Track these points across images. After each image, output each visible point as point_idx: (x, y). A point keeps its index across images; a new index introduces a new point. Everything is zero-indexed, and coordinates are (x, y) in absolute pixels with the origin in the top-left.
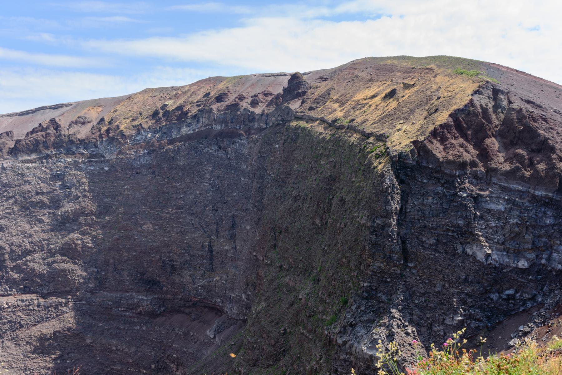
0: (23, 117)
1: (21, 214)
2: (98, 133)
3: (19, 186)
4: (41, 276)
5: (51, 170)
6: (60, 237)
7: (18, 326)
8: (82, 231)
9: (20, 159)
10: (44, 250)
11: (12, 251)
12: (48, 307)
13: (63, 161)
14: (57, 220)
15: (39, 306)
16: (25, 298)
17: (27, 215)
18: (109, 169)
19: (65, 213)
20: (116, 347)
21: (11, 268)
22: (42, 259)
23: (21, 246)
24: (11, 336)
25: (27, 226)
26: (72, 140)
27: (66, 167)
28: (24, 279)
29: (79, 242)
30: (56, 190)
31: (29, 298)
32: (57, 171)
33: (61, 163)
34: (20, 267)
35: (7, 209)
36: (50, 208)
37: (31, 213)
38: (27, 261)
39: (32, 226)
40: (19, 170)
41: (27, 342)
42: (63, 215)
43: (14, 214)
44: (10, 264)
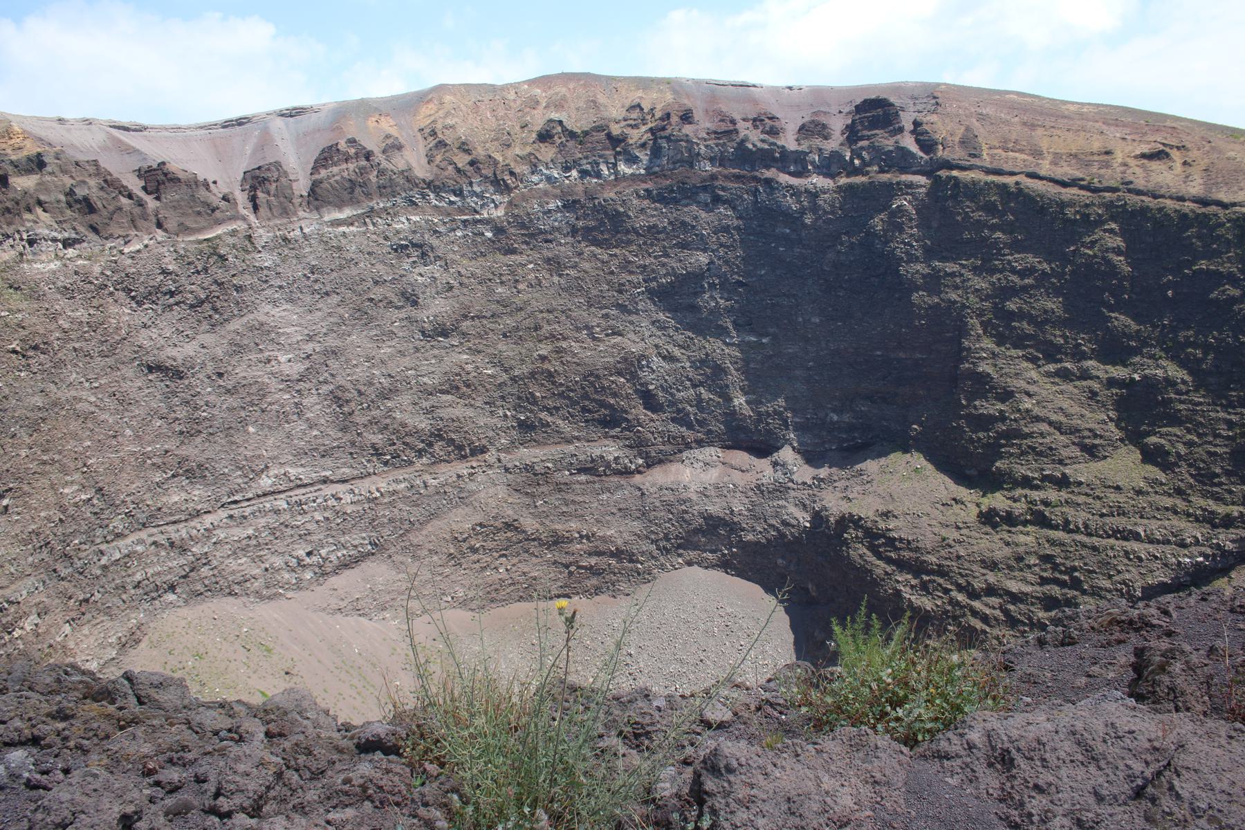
2: (450, 168)
3: (341, 267)
5: (386, 238)
6: (433, 361)
7: (406, 526)
8: (470, 349)
9: (326, 218)
11: (360, 393)
16: (401, 478)
18: (494, 235)
19: (436, 316)
20: (579, 533)
23: (371, 384)
29: (469, 367)
31: (406, 476)
32: (401, 239)
35: (330, 314)
37: (372, 319)
42: (431, 322)
44: (360, 419)
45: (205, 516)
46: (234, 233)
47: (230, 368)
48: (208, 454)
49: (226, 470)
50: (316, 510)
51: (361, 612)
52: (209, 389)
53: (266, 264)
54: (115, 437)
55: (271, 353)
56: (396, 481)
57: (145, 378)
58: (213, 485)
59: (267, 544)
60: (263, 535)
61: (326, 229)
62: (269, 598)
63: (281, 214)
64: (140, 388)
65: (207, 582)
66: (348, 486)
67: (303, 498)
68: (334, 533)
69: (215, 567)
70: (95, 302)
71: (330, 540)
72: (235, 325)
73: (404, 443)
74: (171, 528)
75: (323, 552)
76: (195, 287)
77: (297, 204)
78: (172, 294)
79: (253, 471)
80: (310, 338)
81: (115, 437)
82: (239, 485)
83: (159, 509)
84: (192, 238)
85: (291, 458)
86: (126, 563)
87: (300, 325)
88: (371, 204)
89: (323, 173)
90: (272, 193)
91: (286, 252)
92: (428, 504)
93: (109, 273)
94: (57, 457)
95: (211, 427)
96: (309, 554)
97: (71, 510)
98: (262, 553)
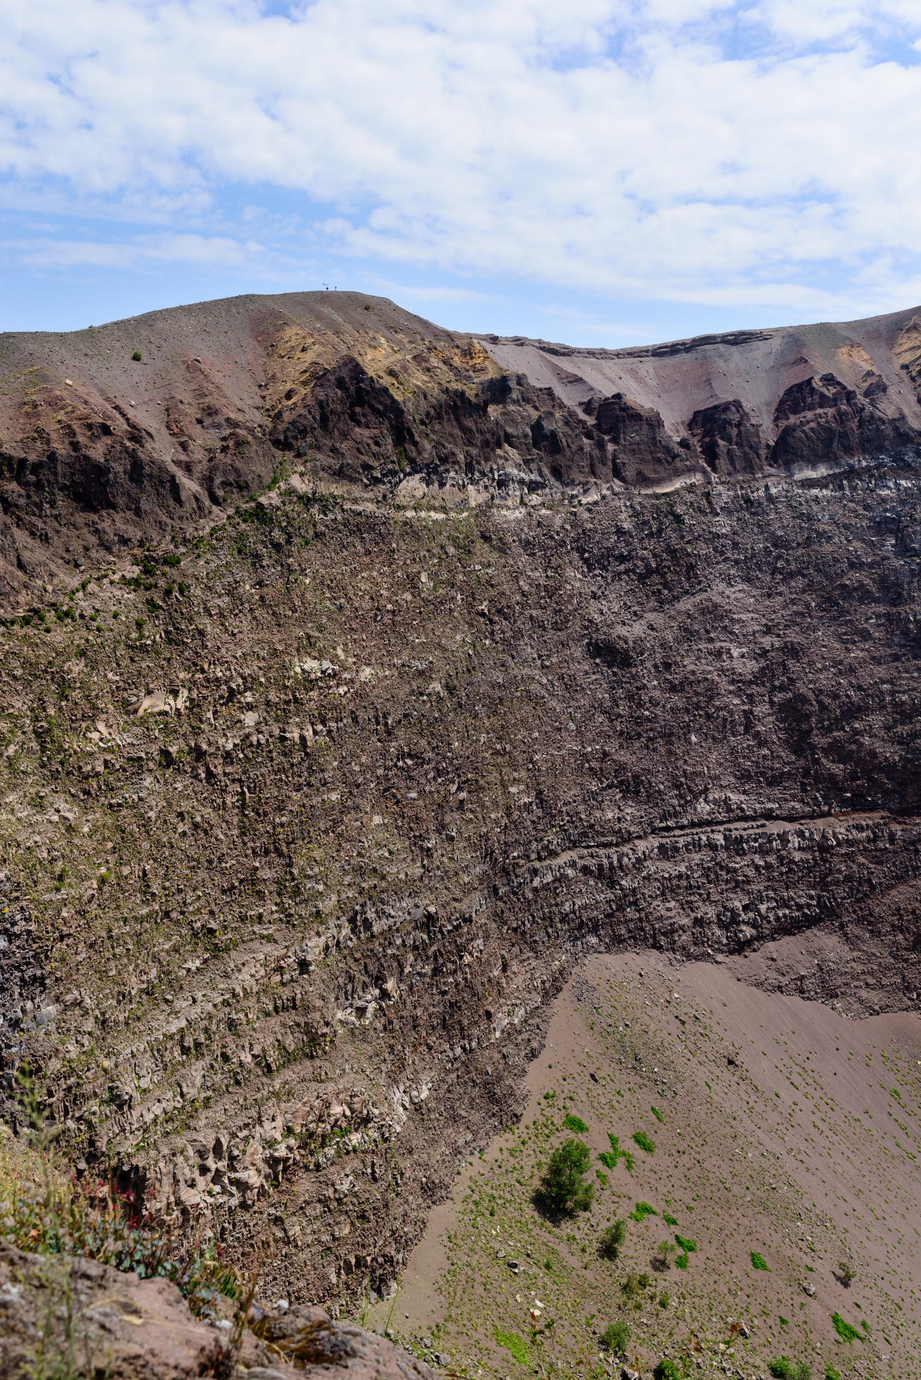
0: (668, 361)
1: (821, 618)
3: (808, 542)
4: (890, 769)
5: (867, 507)
6: (916, 675)
9: (798, 476)
10: (884, 707)
12: (913, 843)
13: (891, 484)
14: (906, 633)
15: (892, 839)
16: (864, 823)
17: (835, 619)
21: (823, 750)
22: (885, 728)
23: (836, 697)
24: (855, 912)
25: (837, 645)
26: (907, 434)
27: (903, 502)
28: (854, 777)
30: (887, 558)
31: (871, 822)
32: (886, 510)
33: (887, 492)
34: (843, 747)
36: (876, 600)
37: (842, 612)
38: (856, 732)
39: (850, 646)
40: (801, 504)
41: (893, 926)
43: (810, 616)
44: (820, 741)
45: (637, 842)
46: (691, 488)
47: (679, 659)
48: (646, 764)
49: (662, 787)
50: (755, 853)
51: (806, 995)
52: (655, 683)
53: (724, 531)
54: (559, 730)
55: (724, 644)
56: (860, 828)
57: (592, 661)
58: (646, 803)
59: (699, 888)
60: (696, 875)
61: (796, 491)
62: (697, 958)
63: (745, 468)
64: (587, 673)
65: (632, 926)
66: (795, 826)
67: (744, 833)
68: (776, 885)
69: (643, 909)
70: (554, 563)
71: (771, 894)
72: (686, 604)
73: (870, 779)
74: (602, 852)
75: (763, 908)
76: (646, 551)
77: (763, 457)
78: (622, 559)
79: (691, 792)
80: (768, 630)
81: (559, 730)
82: (674, 807)
83: (592, 826)
84: (649, 491)
85: (733, 780)
86: (556, 888)
87: (755, 611)
88: (851, 462)
89: (793, 420)
90: (734, 440)
91: (748, 516)
92: (894, 864)
93: (568, 527)
94: (508, 747)
95: (651, 730)
96: (746, 908)
97: (515, 816)
98: (693, 898)
